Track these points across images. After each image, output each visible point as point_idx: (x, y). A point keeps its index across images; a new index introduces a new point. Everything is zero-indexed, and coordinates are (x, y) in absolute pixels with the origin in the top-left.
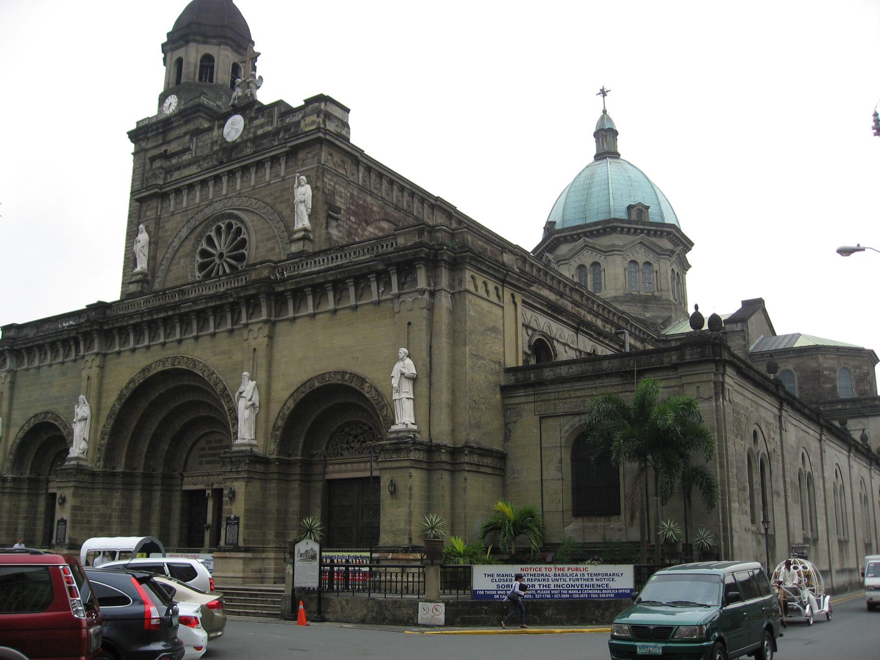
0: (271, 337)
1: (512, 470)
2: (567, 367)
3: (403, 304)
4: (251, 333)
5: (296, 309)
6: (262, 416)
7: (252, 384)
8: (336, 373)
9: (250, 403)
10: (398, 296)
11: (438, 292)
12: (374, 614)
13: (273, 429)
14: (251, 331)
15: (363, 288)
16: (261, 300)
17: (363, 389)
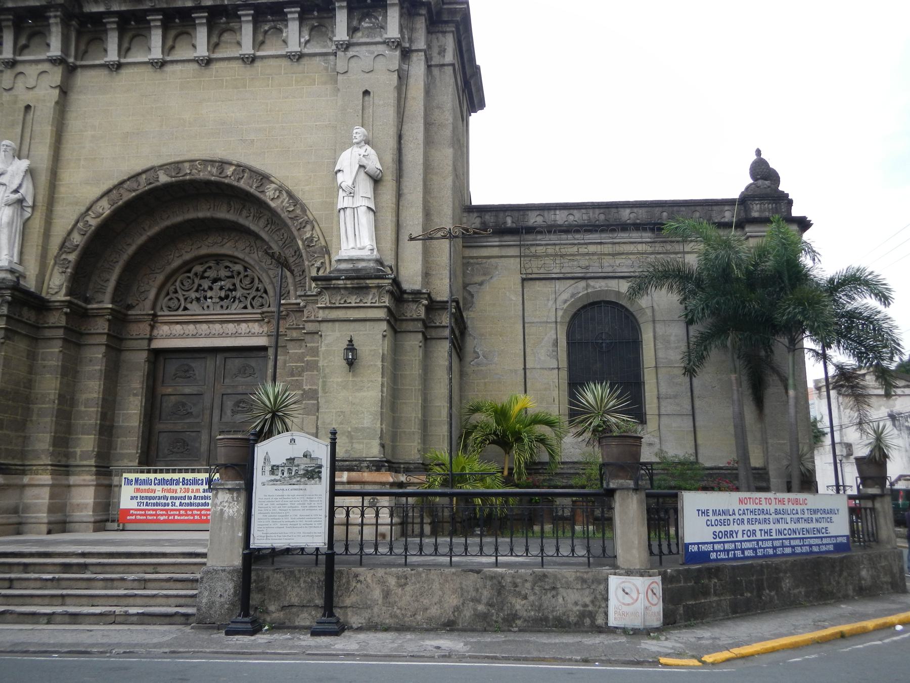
0: (64, 91)
1: (475, 352)
2: (566, 212)
3: (352, 61)
4: (20, 79)
5: (123, 53)
6: (37, 224)
7: (24, 164)
8: (205, 162)
9: (17, 196)
10: (347, 46)
11: (415, 54)
12: (481, 608)
13: (61, 249)
14: (21, 76)
15: (266, 32)
16: (52, 21)
17: (262, 192)
